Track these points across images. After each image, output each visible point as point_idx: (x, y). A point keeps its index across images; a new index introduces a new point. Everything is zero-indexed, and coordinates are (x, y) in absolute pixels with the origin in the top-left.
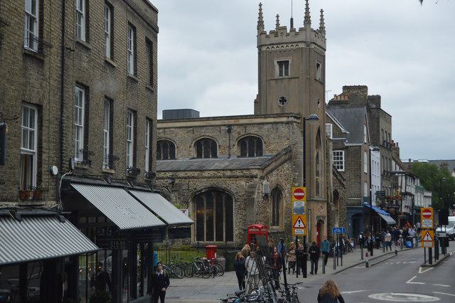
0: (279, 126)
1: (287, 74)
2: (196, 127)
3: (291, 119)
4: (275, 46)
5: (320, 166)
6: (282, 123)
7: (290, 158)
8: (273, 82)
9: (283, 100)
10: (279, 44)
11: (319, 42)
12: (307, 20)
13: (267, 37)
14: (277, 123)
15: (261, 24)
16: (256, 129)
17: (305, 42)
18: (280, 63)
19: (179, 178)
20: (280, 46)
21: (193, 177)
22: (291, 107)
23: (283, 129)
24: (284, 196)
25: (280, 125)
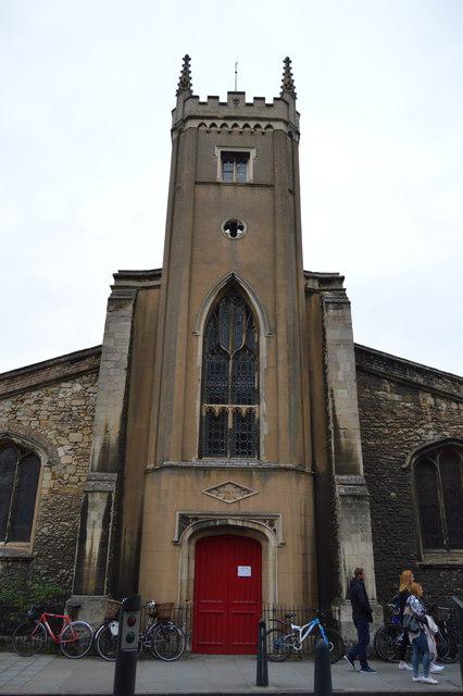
24: (44, 459)
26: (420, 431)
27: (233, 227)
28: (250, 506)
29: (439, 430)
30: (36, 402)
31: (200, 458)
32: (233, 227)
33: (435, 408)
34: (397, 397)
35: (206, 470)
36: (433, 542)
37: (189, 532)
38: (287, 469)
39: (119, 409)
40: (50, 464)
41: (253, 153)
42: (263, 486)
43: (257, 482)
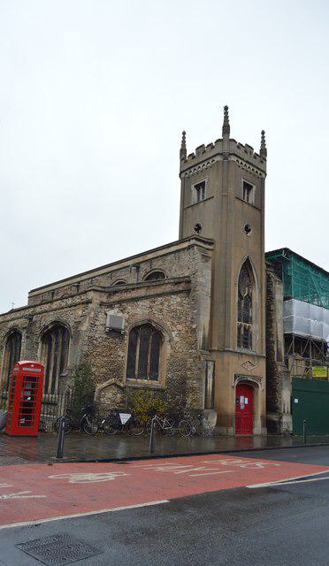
0: (181, 253)
1: (203, 196)
2: (113, 271)
3: (193, 242)
4: (192, 170)
5: (254, 309)
6: (184, 249)
7: (188, 291)
8: (190, 210)
9: (198, 228)
10: (196, 165)
11: (256, 162)
12: (226, 129)
13: (186, 161)
14: (178, 251)
15: (183, 151)
16: (160, 263)
17: (217, 154)
18: (197, 187)
19: (37, 314)
20: (196, 168)
21: (46, 312)
22: (205, 234)
23: (185, 256)
24: (167, 338)
25: (181, 253)
27: (247, 230)
30: (161, 304)
32: (247, 230)
35: (241, 354)
37: (237, 382)
39: (208, 318)
40: (170, 341)
41: (254, 188)
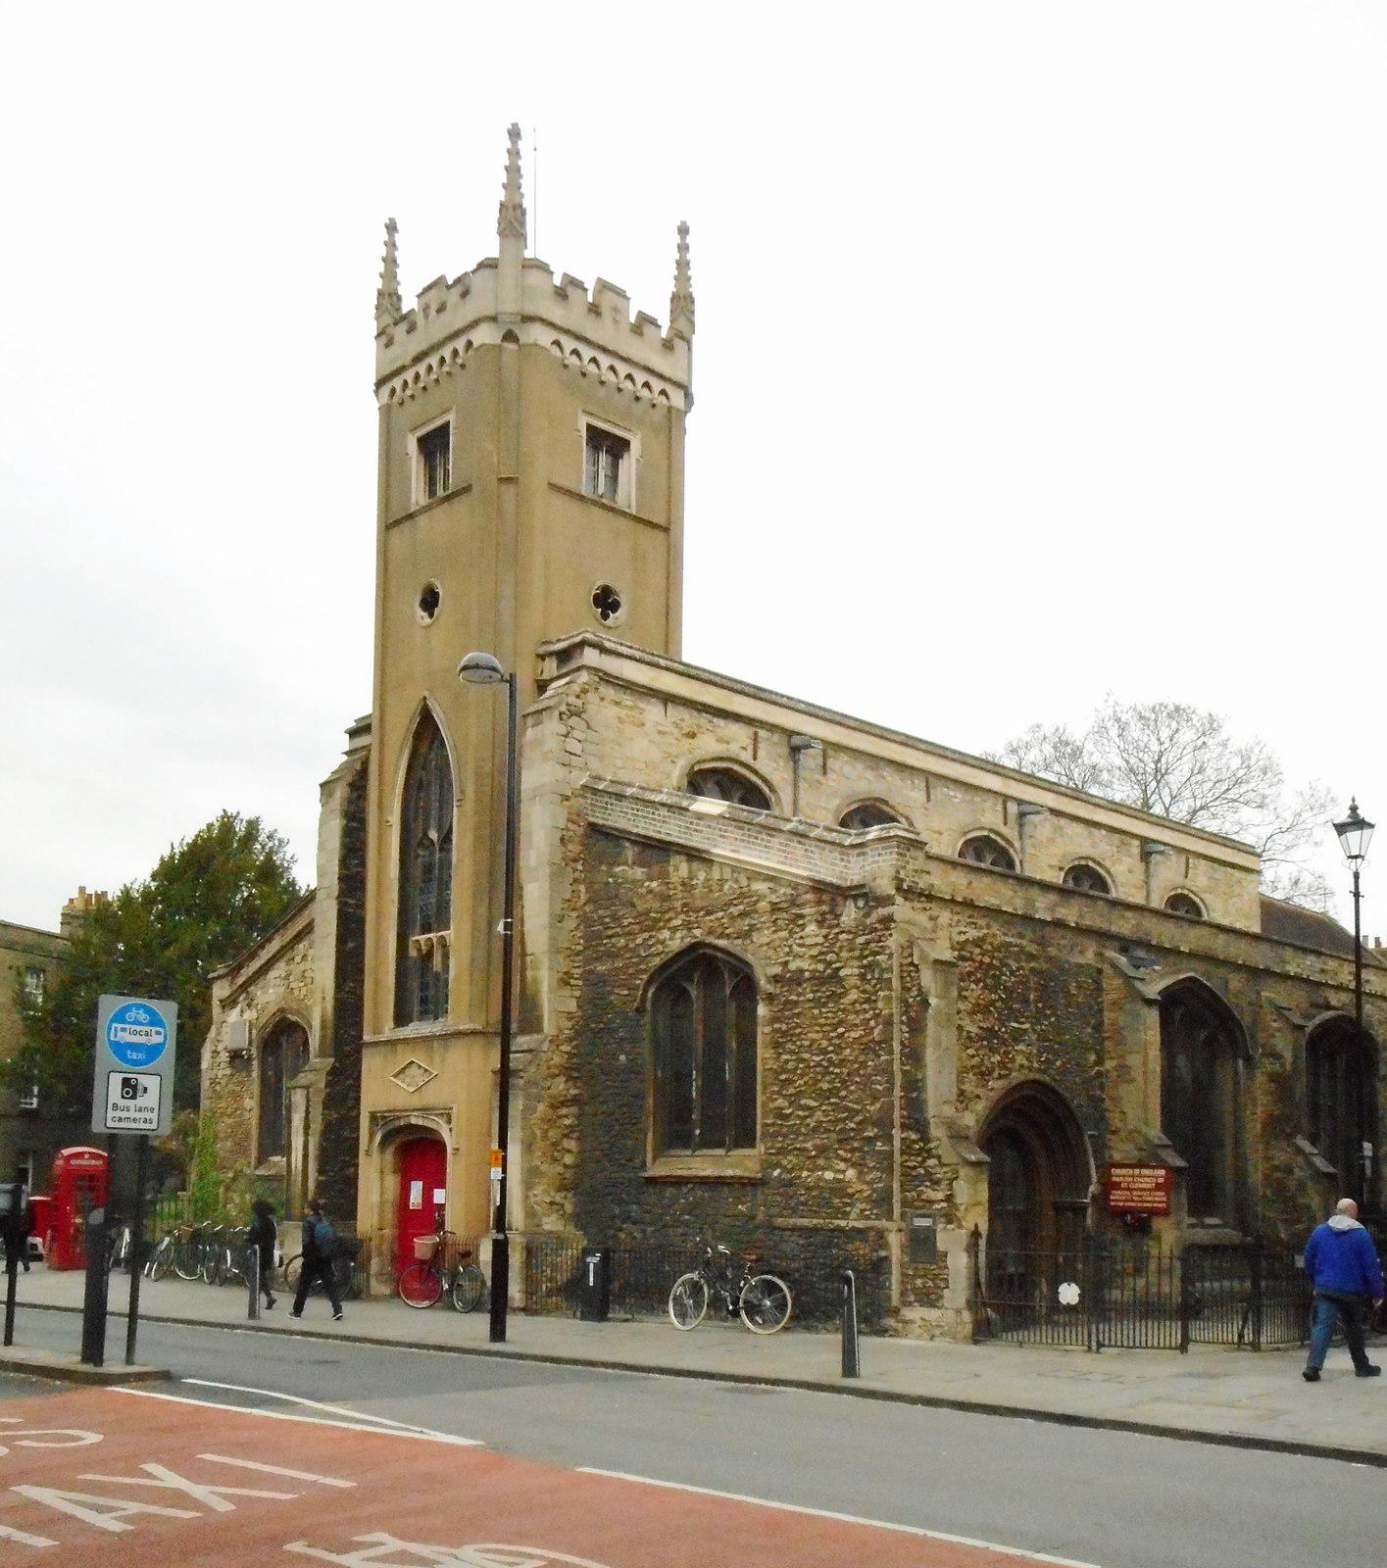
26: (666, 934)
28: (430, 1097)
29: (688, 926)
31: (401, 1019)
33: (687, 886)
34: (639, 873)
36: (677, 1137)
38: (474, 1033)
42: (443, 1061)
43: (437, 1059)
